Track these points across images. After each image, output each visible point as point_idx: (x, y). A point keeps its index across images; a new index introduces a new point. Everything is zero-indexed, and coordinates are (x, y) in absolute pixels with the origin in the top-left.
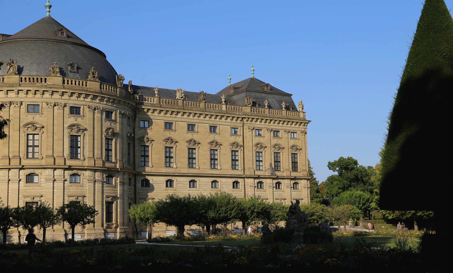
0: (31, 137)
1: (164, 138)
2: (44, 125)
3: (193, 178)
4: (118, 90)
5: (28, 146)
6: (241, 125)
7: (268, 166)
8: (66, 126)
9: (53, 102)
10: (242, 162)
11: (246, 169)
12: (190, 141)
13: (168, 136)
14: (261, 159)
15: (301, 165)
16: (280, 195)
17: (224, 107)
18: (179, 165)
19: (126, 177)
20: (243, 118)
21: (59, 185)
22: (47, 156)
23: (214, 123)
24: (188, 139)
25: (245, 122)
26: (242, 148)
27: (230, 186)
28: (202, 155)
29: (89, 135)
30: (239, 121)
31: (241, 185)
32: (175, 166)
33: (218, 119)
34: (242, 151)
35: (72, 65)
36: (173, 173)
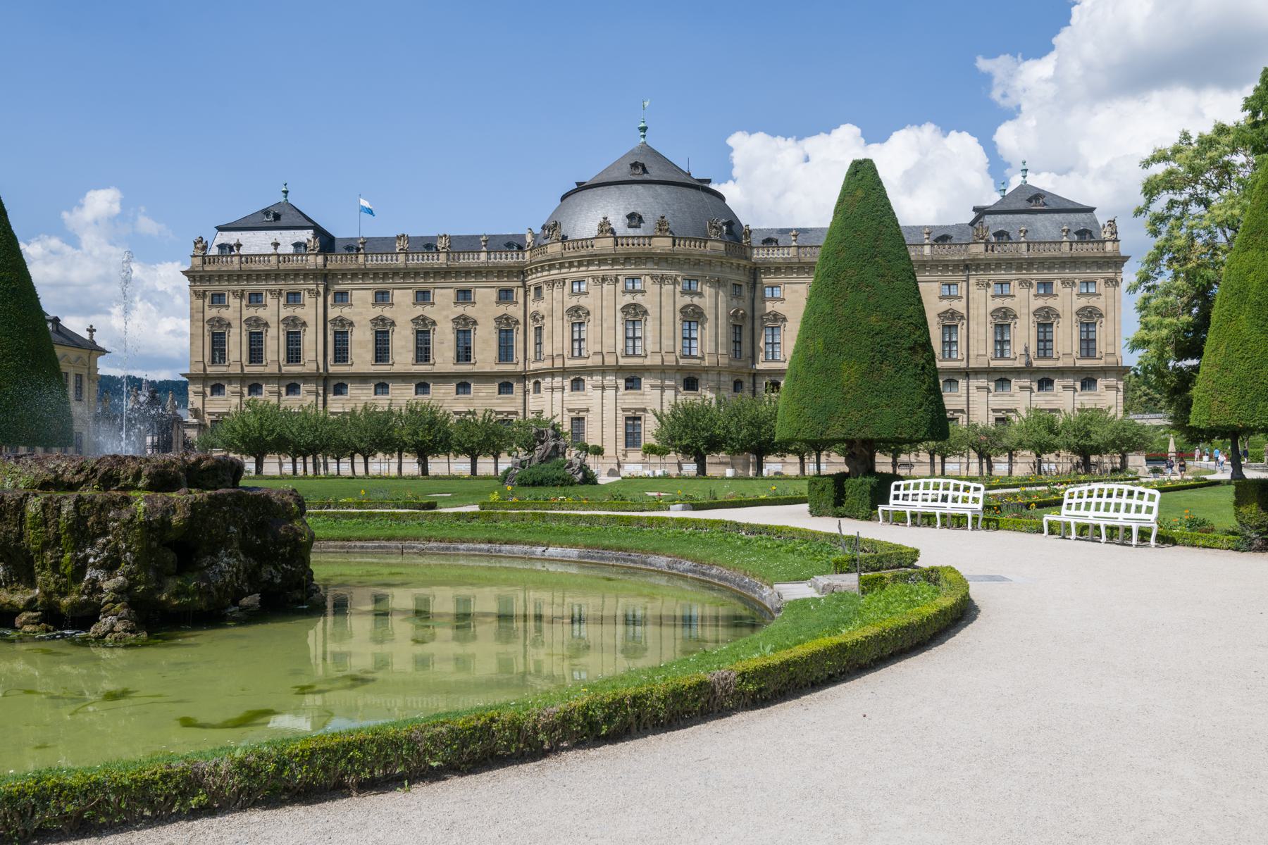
0: (576, 329)
2: (590, 308)
4: (709, 244)
5: (573, 340)
6: (964, 278)
7: (1019, 349)
8: (619, 307)
9: (600, 273)
10: (965, 344)
15: (1103, 344)
16: (1047, 402)
17: (927, 250)
19: (727, 380)
21: (610, 393)
22: (595, 353)
29: (654, 319)
35: (631, 216)
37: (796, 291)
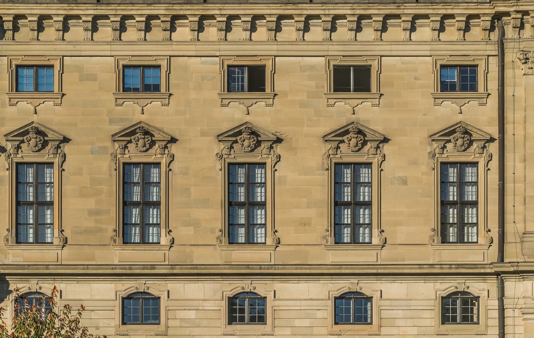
1: (116, 128)
3: (245, 285)
6: (493, 49)
11: (509, 238)
12: (233, 136)
13: (138, 117)
14: (470, 197)
18: (182, 233)
20: (498, 16)
23: (354, 49)
24: (226, 126)
25: (510, 33)
26: (493, 148)
27: (427, 314)
28: (298, 187)
30: (476, 32)
31: (488, 307)
32: (164, 240)
33: (368, 33)
34: (495, 164)
36: (145, 267)
37: (92, 78)
